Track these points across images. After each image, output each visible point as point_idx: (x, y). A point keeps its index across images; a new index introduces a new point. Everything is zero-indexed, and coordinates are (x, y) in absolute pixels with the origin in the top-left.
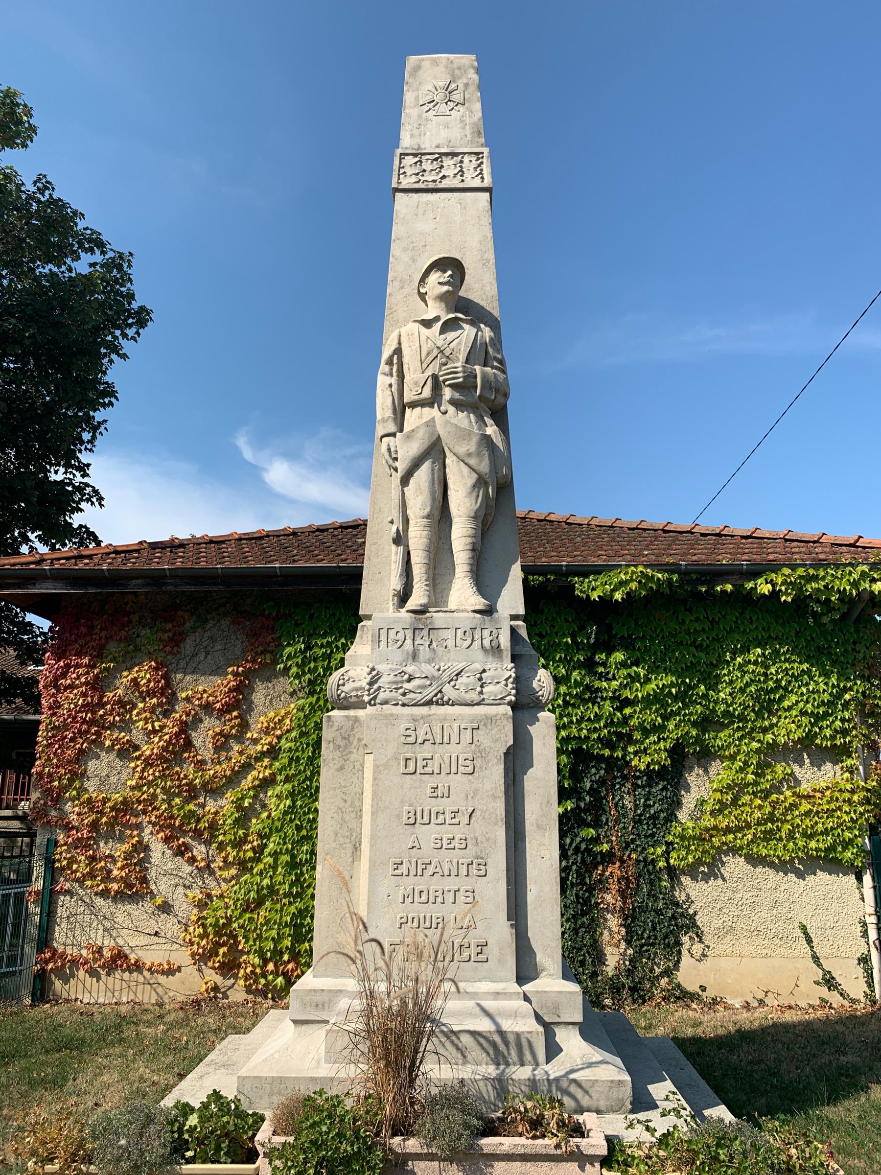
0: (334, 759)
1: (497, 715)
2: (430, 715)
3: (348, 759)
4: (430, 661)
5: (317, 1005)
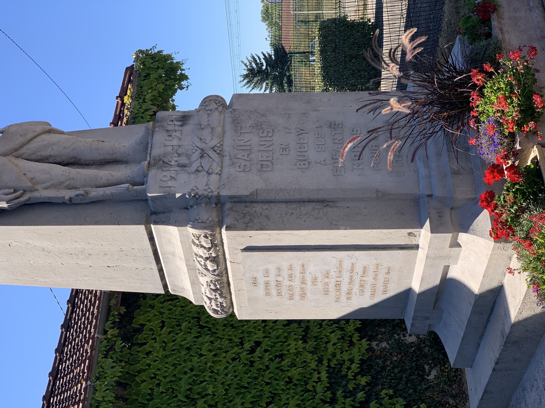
0: (260, 223)
1: (232, 118)
2: (230, 155)
3: (261, 213)
4: (188, 156)
5: (440, 216)
